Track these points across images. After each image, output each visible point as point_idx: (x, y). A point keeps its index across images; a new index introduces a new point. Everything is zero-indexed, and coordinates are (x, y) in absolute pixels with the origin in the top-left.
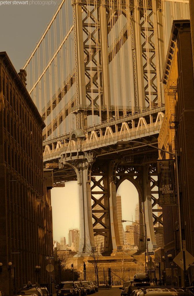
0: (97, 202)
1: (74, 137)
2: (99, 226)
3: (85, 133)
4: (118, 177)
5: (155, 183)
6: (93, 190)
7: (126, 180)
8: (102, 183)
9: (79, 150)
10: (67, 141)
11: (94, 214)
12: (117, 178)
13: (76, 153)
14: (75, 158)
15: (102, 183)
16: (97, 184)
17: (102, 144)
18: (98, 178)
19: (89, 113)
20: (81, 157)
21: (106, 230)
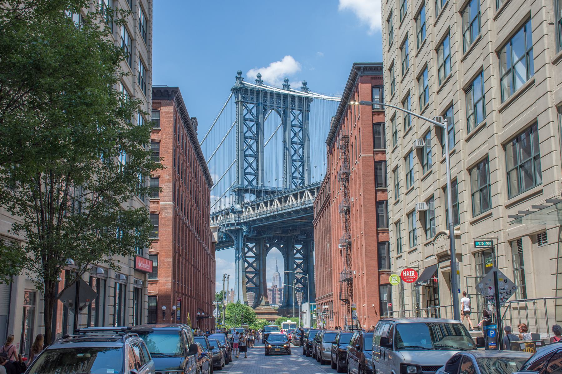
0: (250, 265)
2: (250, 285)
4: (268, 245)
5: (298, 251)
6: (247, 255)
8: (254, 249)
9: (237, 222)
10: (227, 214)
11: (247, 274)
13: (234, 223)
14: (233, 228)
15: (254, 249)
16: (250, 250)
17: (256, 216)
18: (251, 246)
19: (246, 191)
20: (238, 227)
21: (257, 288)
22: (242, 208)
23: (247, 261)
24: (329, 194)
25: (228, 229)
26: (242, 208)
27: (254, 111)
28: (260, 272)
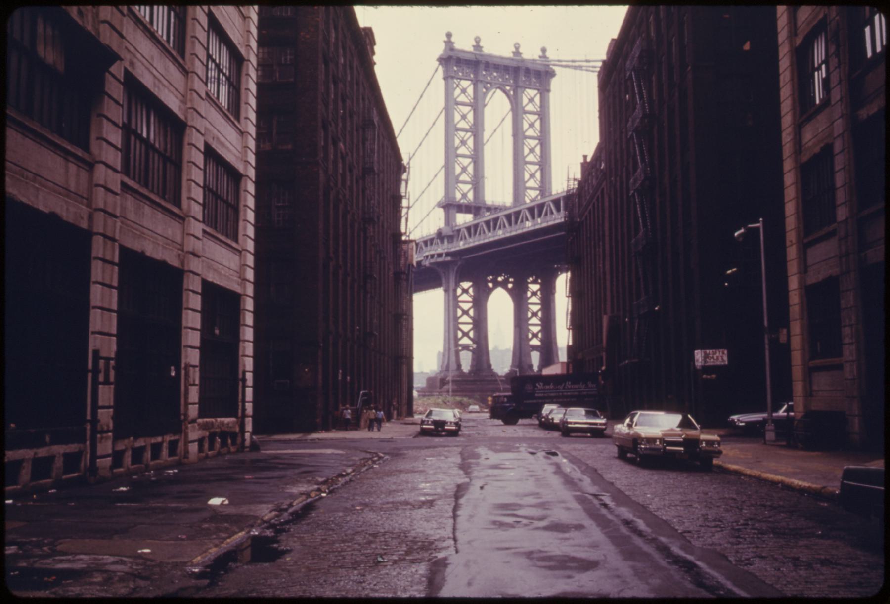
0: (465, 313)
4: (491, 285)
5: (534, 294)
14: (440, 260)
16: (465, 291)
23: (460, 307)
25: (433, 261)
27: (470, 91)
28: (480, 323)
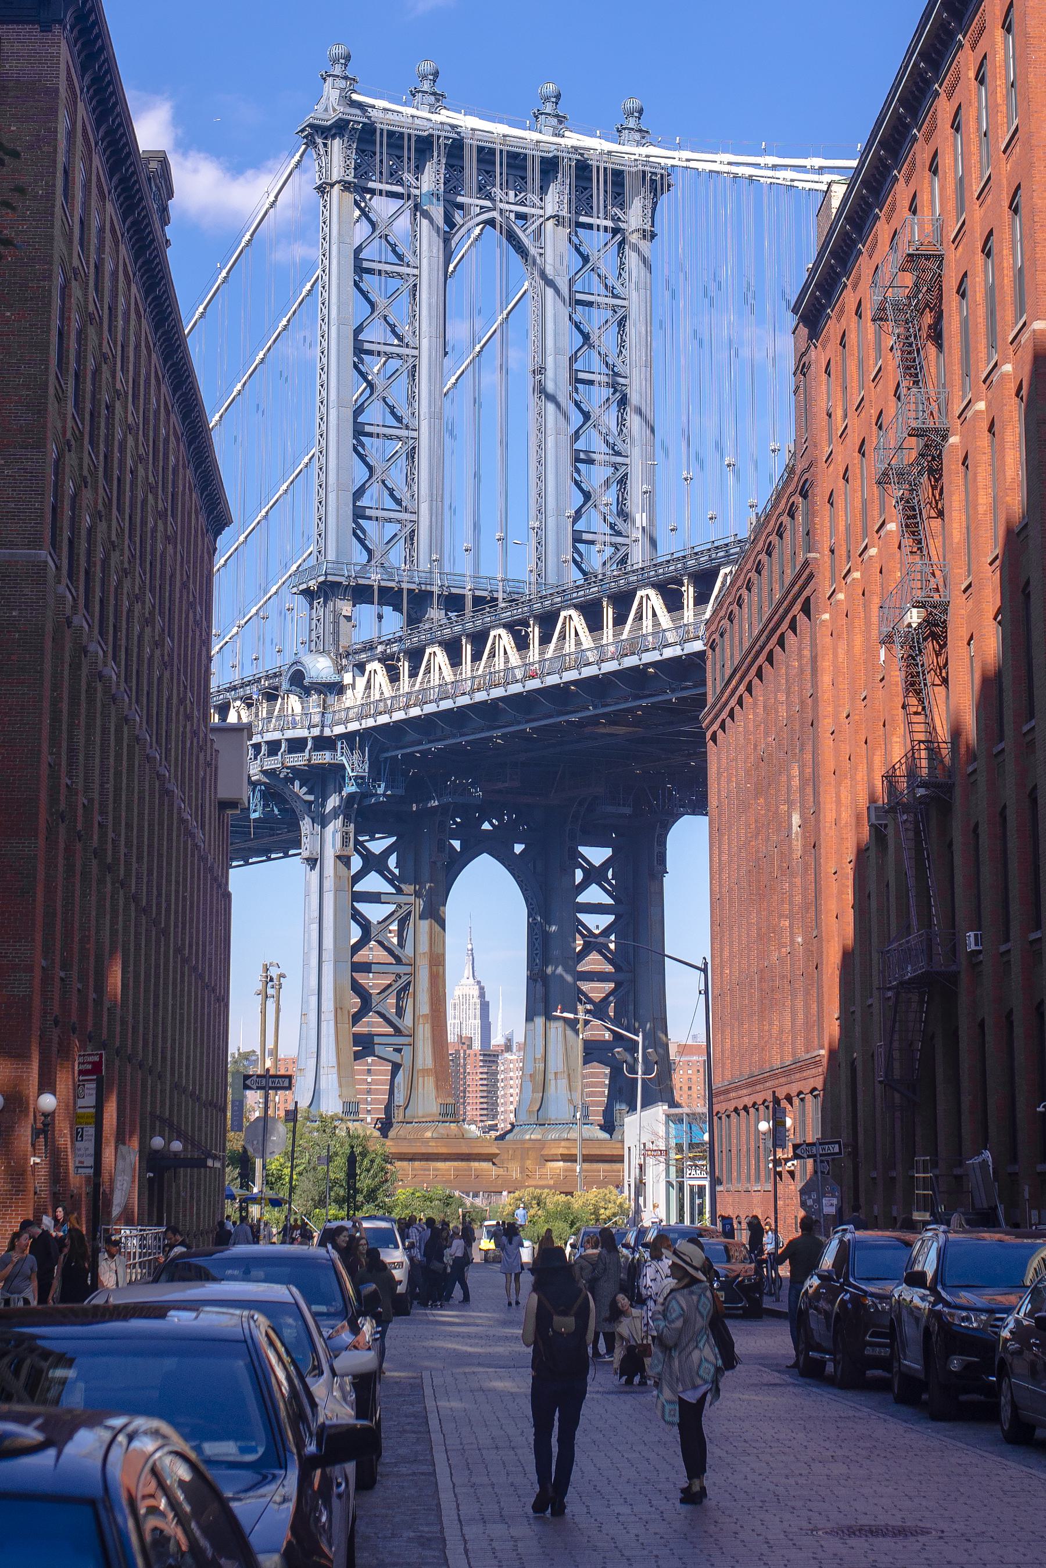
1: (298, 679)
3: (342, 669)
4: (457, 844)
7: (485, 857)
12: (452, 846)
17: (407, 706)
22: (340, 670)
24: (806, 563)
26: (340, 670)
